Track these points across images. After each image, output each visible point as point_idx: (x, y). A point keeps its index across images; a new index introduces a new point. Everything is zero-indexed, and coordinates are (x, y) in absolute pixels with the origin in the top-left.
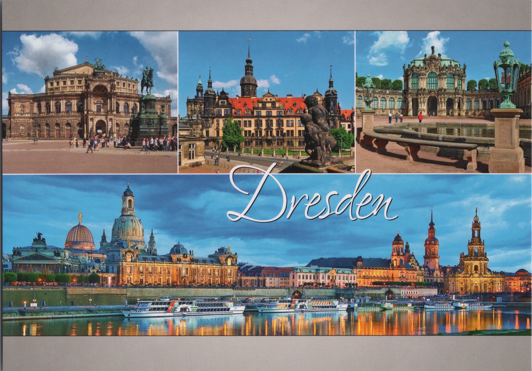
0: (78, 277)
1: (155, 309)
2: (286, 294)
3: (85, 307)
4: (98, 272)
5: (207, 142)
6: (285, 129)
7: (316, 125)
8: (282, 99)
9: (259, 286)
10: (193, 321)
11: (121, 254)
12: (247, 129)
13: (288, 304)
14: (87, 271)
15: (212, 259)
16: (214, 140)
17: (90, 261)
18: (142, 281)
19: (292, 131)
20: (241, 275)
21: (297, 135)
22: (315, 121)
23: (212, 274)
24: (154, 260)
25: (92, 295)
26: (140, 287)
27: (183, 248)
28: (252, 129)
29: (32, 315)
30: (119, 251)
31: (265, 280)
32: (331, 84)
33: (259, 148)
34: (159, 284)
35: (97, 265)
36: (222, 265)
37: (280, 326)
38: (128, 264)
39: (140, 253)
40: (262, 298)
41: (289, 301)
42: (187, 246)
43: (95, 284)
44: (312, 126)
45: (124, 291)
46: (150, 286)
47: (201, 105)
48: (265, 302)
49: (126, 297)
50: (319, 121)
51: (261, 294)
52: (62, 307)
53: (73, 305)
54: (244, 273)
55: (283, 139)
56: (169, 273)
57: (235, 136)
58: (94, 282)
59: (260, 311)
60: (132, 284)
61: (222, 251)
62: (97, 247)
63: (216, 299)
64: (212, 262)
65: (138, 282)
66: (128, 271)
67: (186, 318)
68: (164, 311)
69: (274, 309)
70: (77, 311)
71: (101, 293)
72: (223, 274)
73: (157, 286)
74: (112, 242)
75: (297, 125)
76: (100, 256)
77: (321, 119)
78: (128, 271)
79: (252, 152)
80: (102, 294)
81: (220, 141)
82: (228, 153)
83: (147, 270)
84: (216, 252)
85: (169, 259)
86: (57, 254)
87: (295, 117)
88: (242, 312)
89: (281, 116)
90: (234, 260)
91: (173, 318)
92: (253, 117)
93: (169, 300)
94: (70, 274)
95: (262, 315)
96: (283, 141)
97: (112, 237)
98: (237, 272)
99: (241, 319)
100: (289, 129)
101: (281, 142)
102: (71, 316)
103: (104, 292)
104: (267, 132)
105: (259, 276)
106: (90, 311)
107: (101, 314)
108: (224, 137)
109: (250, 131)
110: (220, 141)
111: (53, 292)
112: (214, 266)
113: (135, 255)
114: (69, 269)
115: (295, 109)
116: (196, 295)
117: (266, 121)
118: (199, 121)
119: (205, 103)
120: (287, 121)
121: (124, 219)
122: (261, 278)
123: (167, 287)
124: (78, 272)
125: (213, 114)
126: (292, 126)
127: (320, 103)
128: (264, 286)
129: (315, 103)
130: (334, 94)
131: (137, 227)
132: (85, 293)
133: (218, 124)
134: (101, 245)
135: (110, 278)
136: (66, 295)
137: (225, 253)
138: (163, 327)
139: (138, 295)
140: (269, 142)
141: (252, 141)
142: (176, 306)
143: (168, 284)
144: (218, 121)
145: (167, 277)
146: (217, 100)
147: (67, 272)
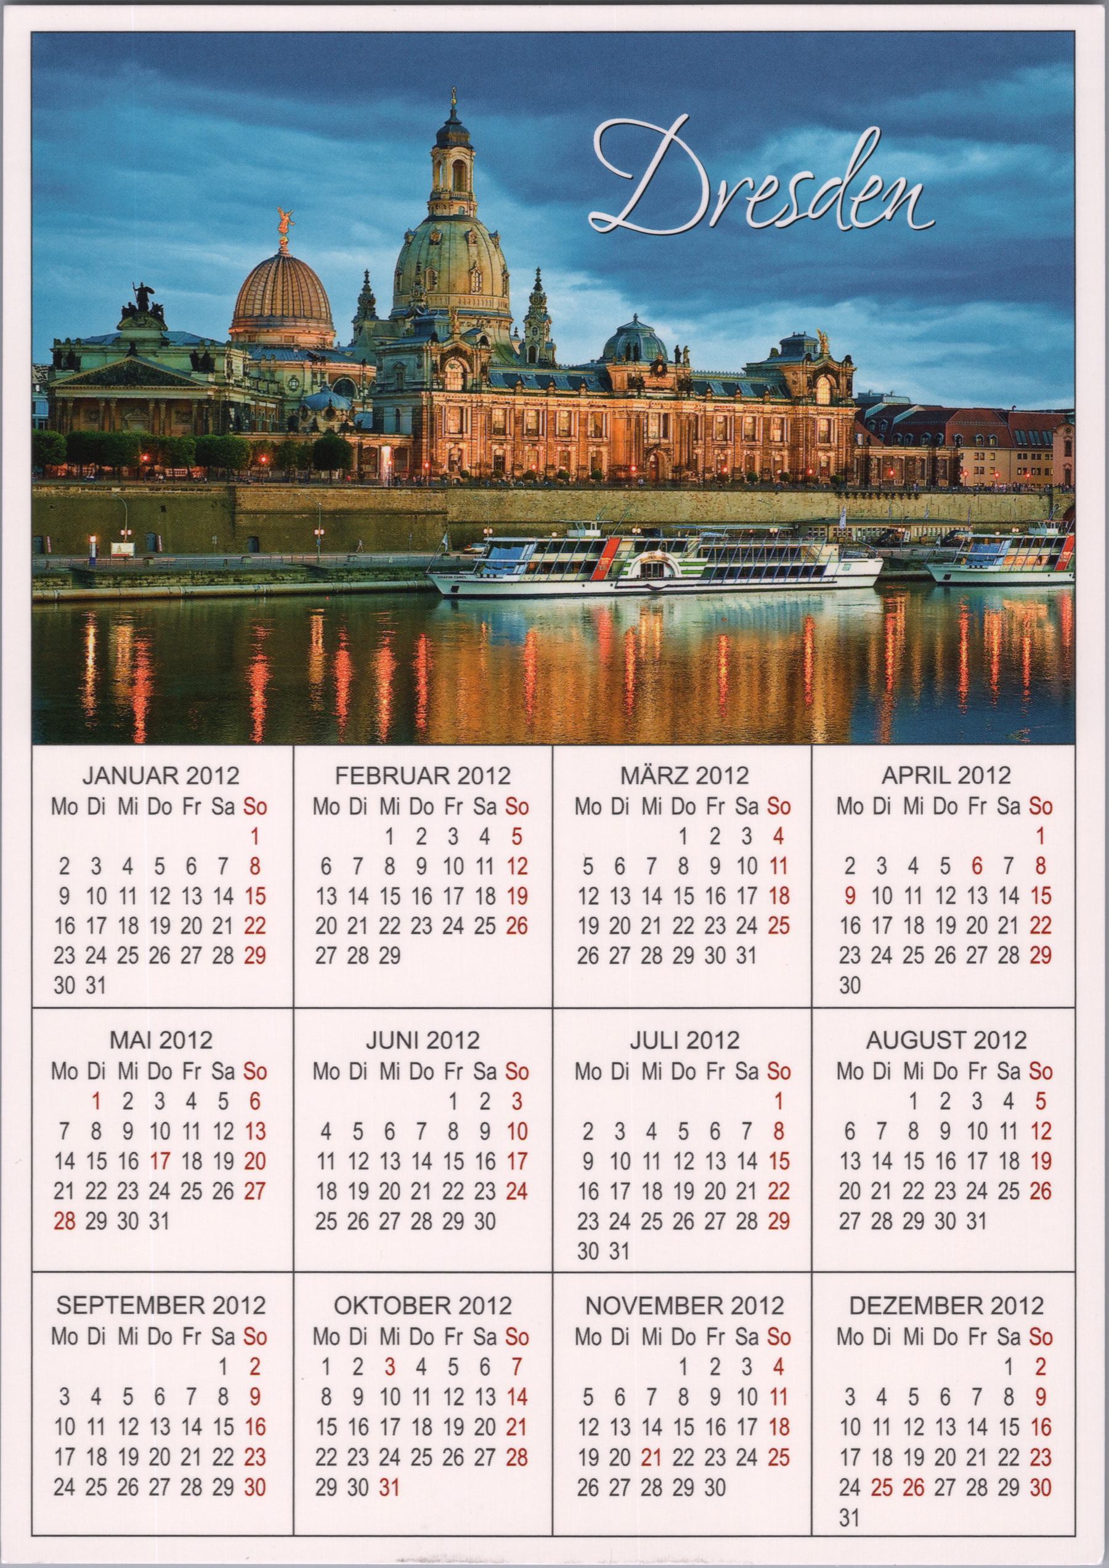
0: (275, 448)
1: (547, 568)
2: (1039, 514)
3: (299, 557)
4: (345, 428)
9: (933, 482)
10: (686, 614)
11: (427, 363)
13: (1046, 552)
14: (307, 424)
15: (760, 381)
17: (317, 389)
18: (500, 462)
20: (868, 442)
23: (759, 435)
24: (545, 383)
25: (324, 513)
26: (494, 486)
27: (653, 339)
29: (117, 585)
30: (419, 351)
31: (956, 460)
34: (561, 475)
35: (342, 404)
36: (796, 401)
37: (1016, 638)
38: (450, 400)
39: (495, 359)
40: (945, 530)
41: (1049, 543)
42: (668, 334)
43: (337, 474)
45: (436, 500)
46: (529, 480)
48: (957, 544)
49: (446, 523)
51: (945, 514)
52: (219, 558)
53: (256, 549)
54: (876, 433)
56: (598, 432)
58: (331, 467)
59: (939, 578)
60: (464, 474)
61: (794, 346)
62: (344, 335)
63: (774, 529)
64: (760, 391)
65: (489, 466)
66: (452, 424)
67: (663, 600)
68: (581, 576)
69: (995, 571)
70: (274, 573)
71: (358, 506)
72: (800, 438)
73: (557, 481)
74: (395, 318)
76: (352, 369)
78: (452, 425)
80: (360, 512)
83: (519, 420)
84: (774, 351)
85: (597, 379)
86: (203, 363)
88: (871, 581)
90: (843, 381)
91: (613, 599)
93: (597, 533)
94: (250, 438)
95: (947, 592)
97: (396, 300)
98: (853, 432)
99: (870, 606)
102: (250, 588)
103: (366, 505)
105: (935, 443)
106: (316, 572)
107: (354, 585)
111: (190, 500)
112: (768, 408)
113: (477, 368)
114: (245, 418)
116: (698, 515)
121: (436, 232)
122: (942, 453)
123: (593, 488)
124: (276, 428)
128: (955, 485)
131: (485, 263)
132: (298, 505)
134: (358, 329)
135: (386, 451)
136: (233, 514)
137: (809, 358)
138: (576, 632)
139: (487, 517)
142: (624, 555)
143: (597, 475)
145: (592, 449)
147: (239, 429)
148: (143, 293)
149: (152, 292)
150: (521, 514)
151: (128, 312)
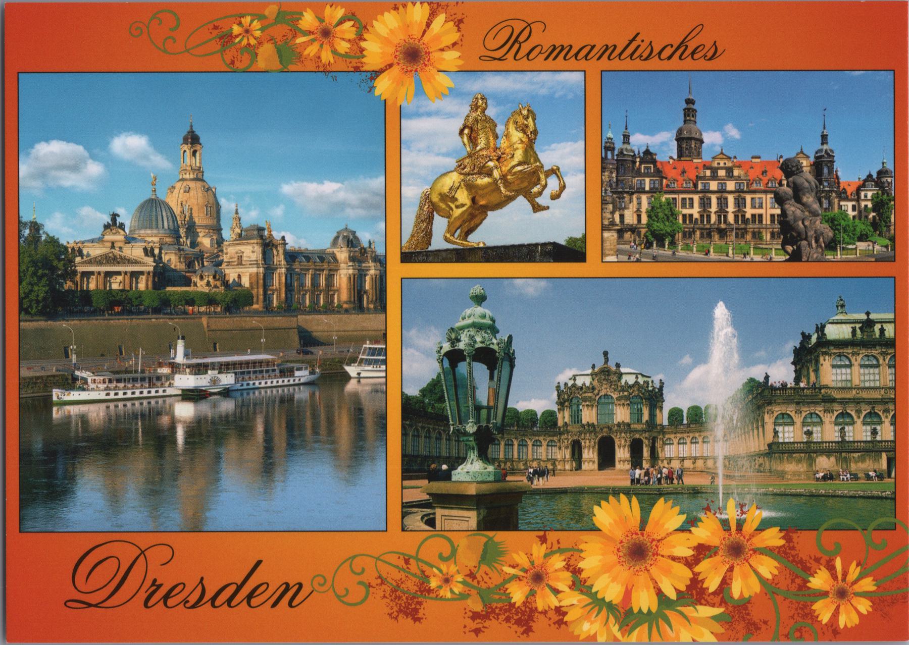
5: (621, 233)
6: (749, 212)
7: (799, 206)
8: (745, 162)
12: (686, 211)
16: (633, 230)
19: (761, 216)
21: (769, 222)
22: (798, 200)
28: (695, 212)
32: (824, 139)
33: (706, 242)
44: (792, 209)
47: (611, 173)
50: (805, 199)
55: (745, 229)
57: (667, 223)
75: (769, 206)
77: (807, 195)
79: (695, 249)
81: (643, 231)
82: (655, 250)
87: (765, 192)
89: (743, 192)
92: (697, 192)
96: (745, 231)
100: (757, 211)
101: (741, 233)
104: (719, 216)
108: (649, 225)
109: (691, 216)
110: (643, 231)
115: (765, 179)
117: (718, 199)
118: (608, 199)
119: (617, 169)
120: (752, 199)
125: (631, 187)
126: (761, 207)
127: (806, 169)
129: (798, 169)
130: (830, 155)
133: (639, 204)
140: (722, 233)
141: (694, 232)
144: (639, 199)
146: (638, 164)
148: (114, 216)
149: (119, 216)
150: (315, 328)
151: (107, 227)
